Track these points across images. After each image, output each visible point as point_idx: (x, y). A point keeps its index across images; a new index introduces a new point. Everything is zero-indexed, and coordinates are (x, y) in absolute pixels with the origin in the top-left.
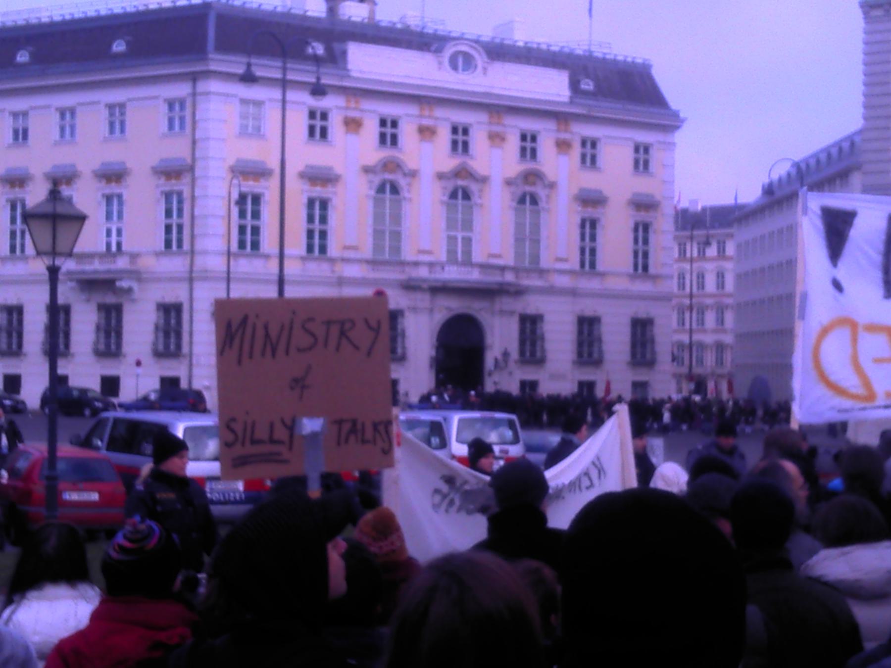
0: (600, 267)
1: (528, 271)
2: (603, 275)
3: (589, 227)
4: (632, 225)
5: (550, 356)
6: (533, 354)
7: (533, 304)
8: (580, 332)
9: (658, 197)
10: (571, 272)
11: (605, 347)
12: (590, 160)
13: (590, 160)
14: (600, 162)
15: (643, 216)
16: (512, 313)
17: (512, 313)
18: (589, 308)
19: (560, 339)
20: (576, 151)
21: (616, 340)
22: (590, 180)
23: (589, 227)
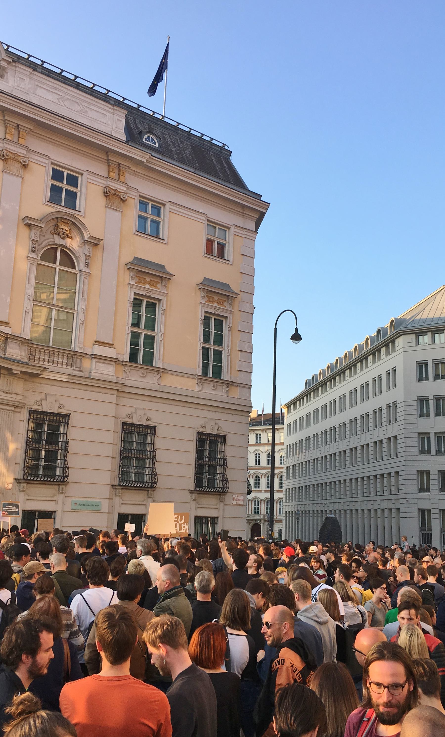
0: (158, 363)
1: (52, 352)
2: (163, 371)
3: (145, 310)
4: (201, 316)
5: (72, 475)
6: (50, 469)
7: (52, 397)
8: (126, 442)
9: (235, 288)
10: (115, 361)
11: (159, 468)
12: (150, 225)
13: (150, 225)
14: (164, 232)
15: (214, 308)
16: (18, 407)
17: (18, 407)
18: (140, 412)
19: (92, 451)
20: (132, 212)
21: (175, 459)
22: (149, 250)
23: (145, 310)
